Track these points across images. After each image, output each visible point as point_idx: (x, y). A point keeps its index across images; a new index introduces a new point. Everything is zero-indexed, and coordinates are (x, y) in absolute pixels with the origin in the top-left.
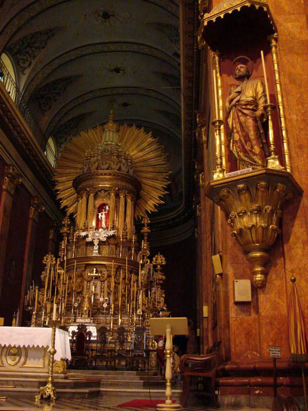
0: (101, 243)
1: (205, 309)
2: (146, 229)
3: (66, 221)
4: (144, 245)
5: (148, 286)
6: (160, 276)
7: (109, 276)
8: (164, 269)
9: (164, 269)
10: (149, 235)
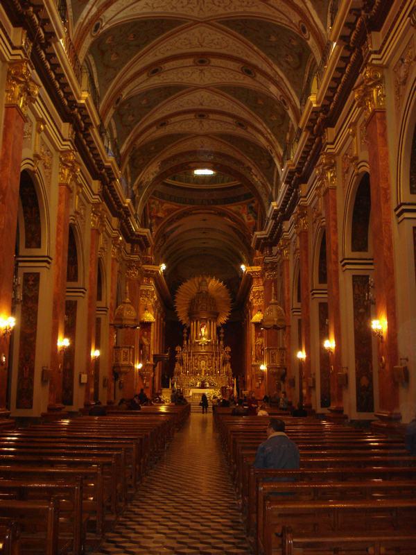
0: (205, 345)
1: (248, 376)
2: (222, 335)
3: (185, 331)
4: (221, 342)
5: (224, 363)
6: (228, 357)
7: (209, 359)
8: (230, 353)
9: (230, 353)
10: (224, 338)
